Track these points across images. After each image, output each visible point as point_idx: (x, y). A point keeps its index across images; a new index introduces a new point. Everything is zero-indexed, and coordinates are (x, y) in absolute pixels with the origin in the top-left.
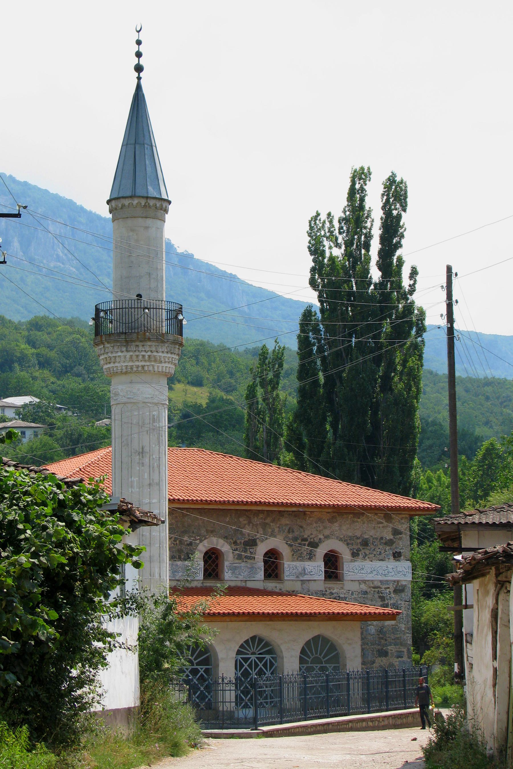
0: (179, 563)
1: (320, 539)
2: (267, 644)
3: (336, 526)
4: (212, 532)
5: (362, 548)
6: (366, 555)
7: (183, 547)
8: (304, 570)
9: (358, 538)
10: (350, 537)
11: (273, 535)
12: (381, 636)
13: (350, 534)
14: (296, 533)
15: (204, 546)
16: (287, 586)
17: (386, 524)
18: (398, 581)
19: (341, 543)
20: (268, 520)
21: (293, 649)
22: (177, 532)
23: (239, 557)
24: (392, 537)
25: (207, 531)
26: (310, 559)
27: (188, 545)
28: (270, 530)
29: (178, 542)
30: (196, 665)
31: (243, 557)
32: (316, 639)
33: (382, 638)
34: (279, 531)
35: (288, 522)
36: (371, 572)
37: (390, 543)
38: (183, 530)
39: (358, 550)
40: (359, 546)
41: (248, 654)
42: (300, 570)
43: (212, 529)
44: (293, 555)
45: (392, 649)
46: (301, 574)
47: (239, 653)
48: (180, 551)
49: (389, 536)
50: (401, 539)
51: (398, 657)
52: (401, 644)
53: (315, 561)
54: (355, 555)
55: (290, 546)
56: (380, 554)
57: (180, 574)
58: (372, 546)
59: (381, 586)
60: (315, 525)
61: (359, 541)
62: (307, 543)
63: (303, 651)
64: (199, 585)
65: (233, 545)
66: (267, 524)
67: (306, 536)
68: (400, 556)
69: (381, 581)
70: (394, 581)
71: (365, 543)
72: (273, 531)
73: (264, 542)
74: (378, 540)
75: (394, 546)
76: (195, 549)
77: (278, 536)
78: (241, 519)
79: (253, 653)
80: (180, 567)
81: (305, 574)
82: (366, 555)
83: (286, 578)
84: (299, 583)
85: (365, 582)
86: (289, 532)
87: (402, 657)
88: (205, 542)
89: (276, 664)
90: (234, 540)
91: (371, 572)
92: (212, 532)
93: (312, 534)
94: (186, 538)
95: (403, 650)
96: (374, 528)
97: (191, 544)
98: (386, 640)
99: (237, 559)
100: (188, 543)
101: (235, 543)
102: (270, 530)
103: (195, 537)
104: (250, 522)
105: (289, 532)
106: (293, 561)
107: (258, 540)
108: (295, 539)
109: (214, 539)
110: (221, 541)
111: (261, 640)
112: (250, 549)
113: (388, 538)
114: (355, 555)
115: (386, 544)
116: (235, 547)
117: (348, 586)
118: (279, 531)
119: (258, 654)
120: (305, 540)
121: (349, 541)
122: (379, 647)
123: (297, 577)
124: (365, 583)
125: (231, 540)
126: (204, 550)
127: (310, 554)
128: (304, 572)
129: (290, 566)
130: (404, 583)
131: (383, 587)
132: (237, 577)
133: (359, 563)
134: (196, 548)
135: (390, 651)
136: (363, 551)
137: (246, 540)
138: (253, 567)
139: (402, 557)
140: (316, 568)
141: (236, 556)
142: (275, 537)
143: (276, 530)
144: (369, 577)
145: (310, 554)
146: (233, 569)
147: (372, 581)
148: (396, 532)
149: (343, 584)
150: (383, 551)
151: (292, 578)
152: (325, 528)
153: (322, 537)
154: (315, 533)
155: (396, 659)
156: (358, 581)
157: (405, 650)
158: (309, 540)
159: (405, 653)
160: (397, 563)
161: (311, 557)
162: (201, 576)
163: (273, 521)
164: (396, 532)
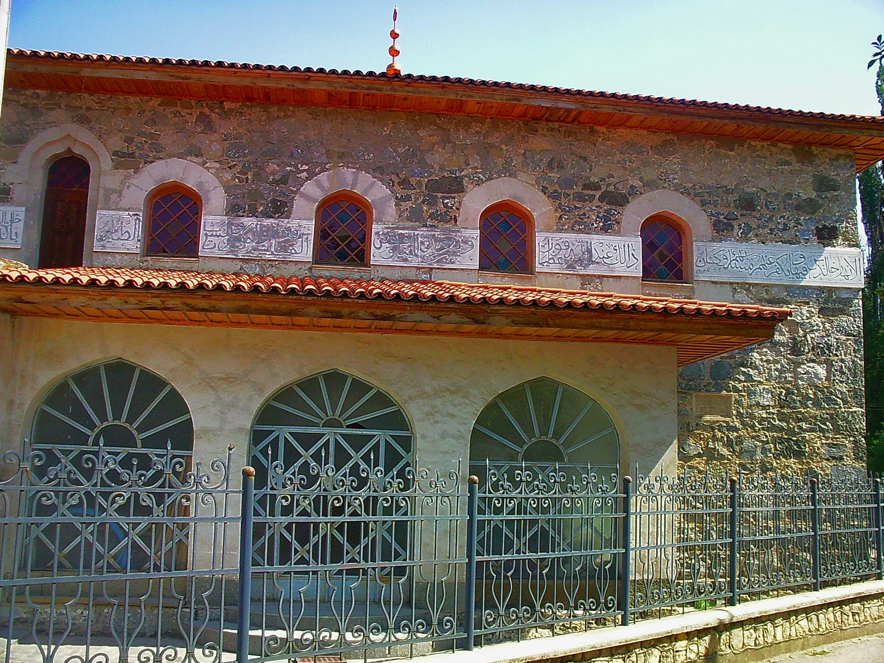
0: (249, 222)
2: (382, 400)
4: (342, 156)
6: (750, 229)
8: (589, 251)
9: (728, 192)
10: (709, 187)
11: (508, 171)
15: (319, 185)
17: (797, 166)
18: (830, 290)
19: (685, 200)
21: (453, 416)
22: (250, 153)
23: (415, 217)
24: (813, 195)
25: (329, 154)
26: (605, 230)
27: (276, 182)
34: (525, 165)
35: (550, 147)
37: (811, 206)
38: (265, 149)
39: (730, 218)
41: (316, 425)
42: (578, 250)
43: (343, 150)
46: (580, 261)
48: (255, 196)
49: (807, 193)
50: (836, 199)
52: (837, 430)
53: (618, 233)
55: (554, 196)
56: (784, 229)
57: (250, 245)
58: (765, 211)
59: (788, 299)
60: (618, 156)
62: (598, 194)
66: (492, 146)
69: (786, 287)
70: (821, 289)
71: (748, 204)
74: (780, 199)
76: (295, 193)
78: (422, 133)
79: (332, 423)
80: (251, 230)
81: (591, 261)
82: (750, 229)
83: (538, 268)
88: (323, 177)
92: (345, 157)
94: (272, 166)
96: (770, 173)
97: (284, 180)
99: (409, 219)
100: (277, 177)
101: (405, 183)
102: (500, 161)
103: (296, 166)
104: (446, 141)
105: (550, 166)
106: (560, 231)
108: (568, 183)
109: (348, 174)
110: (365, 178)
111: (359, 387)
112: (444, 198)
114: (722, 229)
115: (798, 208)
119: (348, 427)
120: (596, 187)
121: (706, 197)
124: (748, 290)
125: (394, 178)
126: (319, 195)
127: (606, 219)
132: (405, 260)
134: (299, 189)
136: (742, 221)
138: (449, 239)
141: (406, 214)
142: (513, 175)
143: (517, 161)
146: (396, 241)
147: (768, 285)
149: (692, 288)
150: (792, 224)
153: (638, 183)
156: (731, 283)
158: (604, 188)
162: (305, 251)
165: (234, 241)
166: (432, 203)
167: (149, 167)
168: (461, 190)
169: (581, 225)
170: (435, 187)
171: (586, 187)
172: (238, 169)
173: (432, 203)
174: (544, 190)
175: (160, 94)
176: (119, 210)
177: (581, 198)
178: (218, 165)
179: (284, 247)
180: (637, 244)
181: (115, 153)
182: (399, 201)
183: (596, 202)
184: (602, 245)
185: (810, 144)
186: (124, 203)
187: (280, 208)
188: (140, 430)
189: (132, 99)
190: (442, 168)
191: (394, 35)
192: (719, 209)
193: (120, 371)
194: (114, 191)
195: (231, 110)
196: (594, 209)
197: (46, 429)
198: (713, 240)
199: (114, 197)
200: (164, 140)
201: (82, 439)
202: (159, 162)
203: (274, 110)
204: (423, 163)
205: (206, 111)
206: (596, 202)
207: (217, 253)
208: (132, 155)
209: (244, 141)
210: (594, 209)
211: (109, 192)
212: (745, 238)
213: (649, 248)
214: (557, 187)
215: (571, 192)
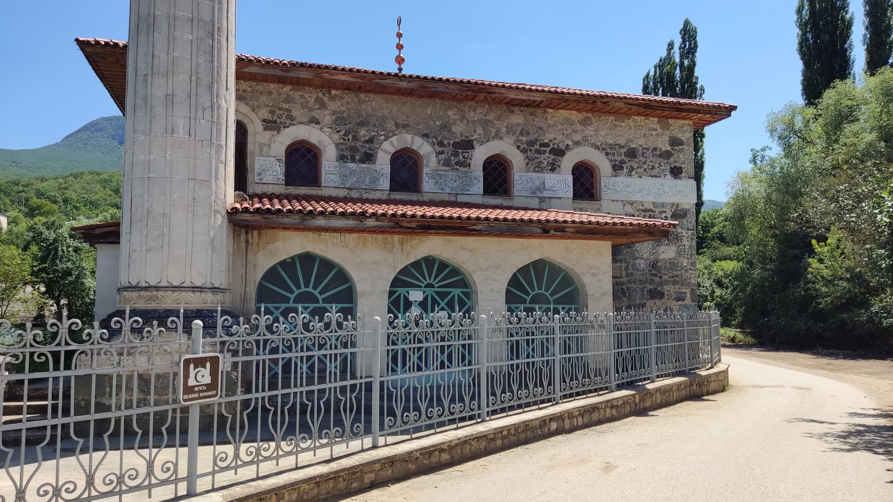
0: (352, 165)
1: (567, 145)
2: (455, 272)
3: (590, 131)
4: (404, 126)
5: (626, 159)
7: (358, 144)
9: (621, 147)
10: (610, 145)
11: (498, 136)
12: (653, 272)
13: (611, 142)
14: (532, 137)
15: (392, 144)
16: (516, 202)
17: (660, 131)
19: (597, 152)
20: (491, 117)
21: (496, 280)
22: (350, 123)
23: (447, 163)
24: (669, 148)
25: (397, 125)
26: (553, 170)
28: (494, 130)
29: (350, 137)
30: (294, 302)
31: (453, 163)
32: (539, 266)
33: (656, 275)
34: (508, 132)
36: (641, 191)
37: (667, 155)
40: (623, 157)
42: (537, 183)
44: (527, 164)
45: (669, 289)
47: (397, 282)
50: (682, 150)
51: (678, 299)
53: (559, 173)
54: (617, 168)
55: (524, 151)
58: (641, 158)
60: (560, 127)
61: (623, 150)
63: (514, 282)
64: (384, 197)
65: (436, 146)
66: (489, 121)
67: (546, 141)
68: (681, 172)
71: (632, 154)
72: (498, 131)
73: (485, 145)
75: (672, 160)
77: (506, 139)
78: (450, 113)
82: (633, 169)
84: (537, 201)
85: (632, 203)
86: (522, 134)
87: (684, 300)
88: (394, 139)
89: (469, 304)
90: (439, 139)
91: (641, 191)
93: (555, 139)
94: (363, 132)
95: (684, 291)
97: (371, 141)
98: (661, 278)
100: (367, 138)
101: (441, 144)
103: (377, 132)
104: (463, 117)
105: (522, 134)
106: (528, 171)
107: (475, 142)
108: (531, 143)
111: (443, 265)
112: (463, 153)
113: (664, 149)
114: (617, 168)
115: (660, 156)
116: (441, 149)
117: (605, 203)
118: (508, 132)
120: (547, 145)
121: (609, 151)
122: (651, 287)
123: (533, 192)
124: (632, 204)
125: (435, 140)
126: (392, 150)
128: (543, 187)
129: (521, 179)
130: (686, 207)
131: (657, 210)
132: (443, 189)
133: (622, 180)
135: (666, 293)
136: (629, 164)
137: (456, 140)
139: (683, 174)
140: (562, 182)
141: (442, 162)
142: (501, 138)
144: (637, 198)
145: (553, 164)
148: (675, 142)
150: (657, 165)
151: (525, 193)
152: (575, 131)
153: (570, 143)
154: (559, 137)
155: (675, 302)
157: (688, 291)
159: (688, 295)
160: (677, 181)
161: (554, 168)
162: (385, 183)
163: (499, 118)
164: (675, 142)
165: (344, 177)
166: (456, 154)
167: (287, 130)
168: (473, 148)
169: (539, 168)
170: (457, 145)
171: (541, 145)
172: (343, 133)
173: (456, 154)
174: (518, 147)
175: (291, 83)
176: (269, 156)
177: (538, 152)
178: (329, 130)
179: (375, 180)
180: (570, 179)
181: (264, 120)
182: (438, 153)
183: (547, 154)
184: (550, 179)
185: (668, 118)
186: (272, 153)
187: (369, 158)
188: (321, 293)
189: (272, 86)
190: (461, 135)
191: (399, 35)
192: (617, 158)
193: (307, 259)
194: (265, 145)
195: (336, 95)
196: (546, 158)
197: (511, 298)
198: (612, 176)
199: (265, 148)
200: (294, 113)
201: (286, 300)
202: (292, 128)
203: (362, 96)
204: (450, 130)
205: (320, 95)
206: (547, 154)
207: (332, 184)
208: (275, 122)
209: (345, 115)
210: (546, 158)
211: (262, 146)
212: (630, 175)
213: (576, 181)
214: (525, 146)
215: (533, 148)
